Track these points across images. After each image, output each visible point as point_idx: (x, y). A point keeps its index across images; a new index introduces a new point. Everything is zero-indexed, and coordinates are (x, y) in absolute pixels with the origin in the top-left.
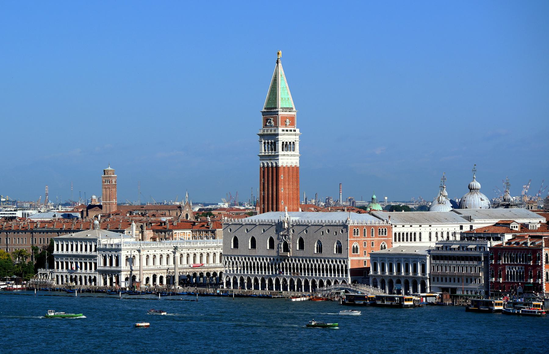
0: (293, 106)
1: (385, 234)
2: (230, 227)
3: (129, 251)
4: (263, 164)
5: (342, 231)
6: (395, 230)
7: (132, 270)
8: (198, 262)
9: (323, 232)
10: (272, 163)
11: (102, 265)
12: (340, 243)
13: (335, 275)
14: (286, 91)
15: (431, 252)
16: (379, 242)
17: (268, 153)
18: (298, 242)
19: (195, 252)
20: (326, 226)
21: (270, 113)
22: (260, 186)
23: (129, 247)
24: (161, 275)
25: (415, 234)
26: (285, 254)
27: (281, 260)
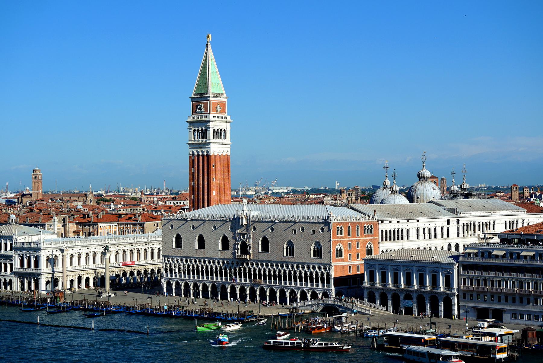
0: (224, 92)
1: (371, 233)
2: (171, 223)
3: (51, 251)
4: (193, 152)
5: (322, 230)
6: (382, 227)
7: (54, 273)
8: (128, 259)
9: (295, 231)
10: (202, 152)
11: (19, 266)
12: (320, 245)
13: (312, 285)
14: (217, 76)
15: (461, 259)
16: (365, 242)
17: (198, 141)
18: (260, 243)
19: (125, 248)
20: (299, 222)
21: (200, 99)
22: (190, 175)
23: (50, 246)
24: (87, 276)
25: (402, 230)
26: (243, 256)
27: (237, 263)
